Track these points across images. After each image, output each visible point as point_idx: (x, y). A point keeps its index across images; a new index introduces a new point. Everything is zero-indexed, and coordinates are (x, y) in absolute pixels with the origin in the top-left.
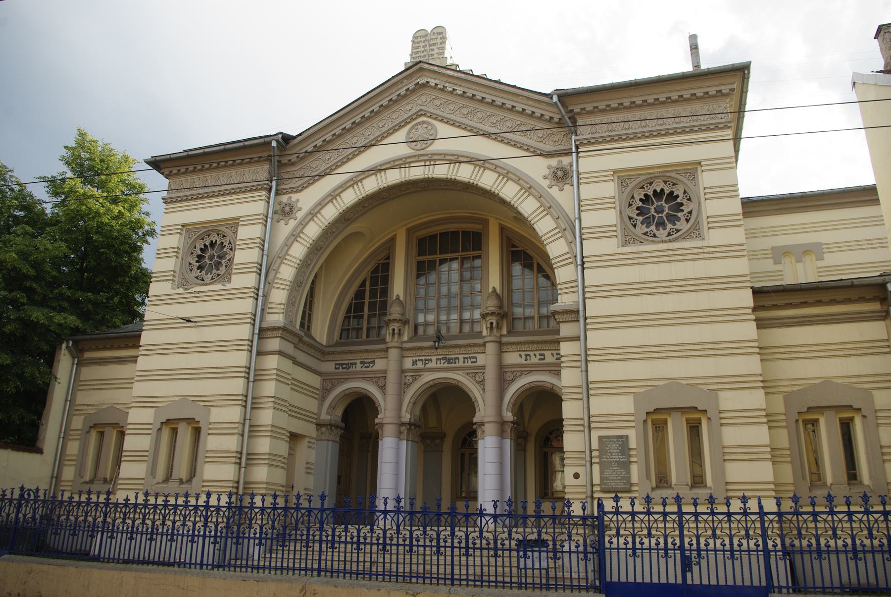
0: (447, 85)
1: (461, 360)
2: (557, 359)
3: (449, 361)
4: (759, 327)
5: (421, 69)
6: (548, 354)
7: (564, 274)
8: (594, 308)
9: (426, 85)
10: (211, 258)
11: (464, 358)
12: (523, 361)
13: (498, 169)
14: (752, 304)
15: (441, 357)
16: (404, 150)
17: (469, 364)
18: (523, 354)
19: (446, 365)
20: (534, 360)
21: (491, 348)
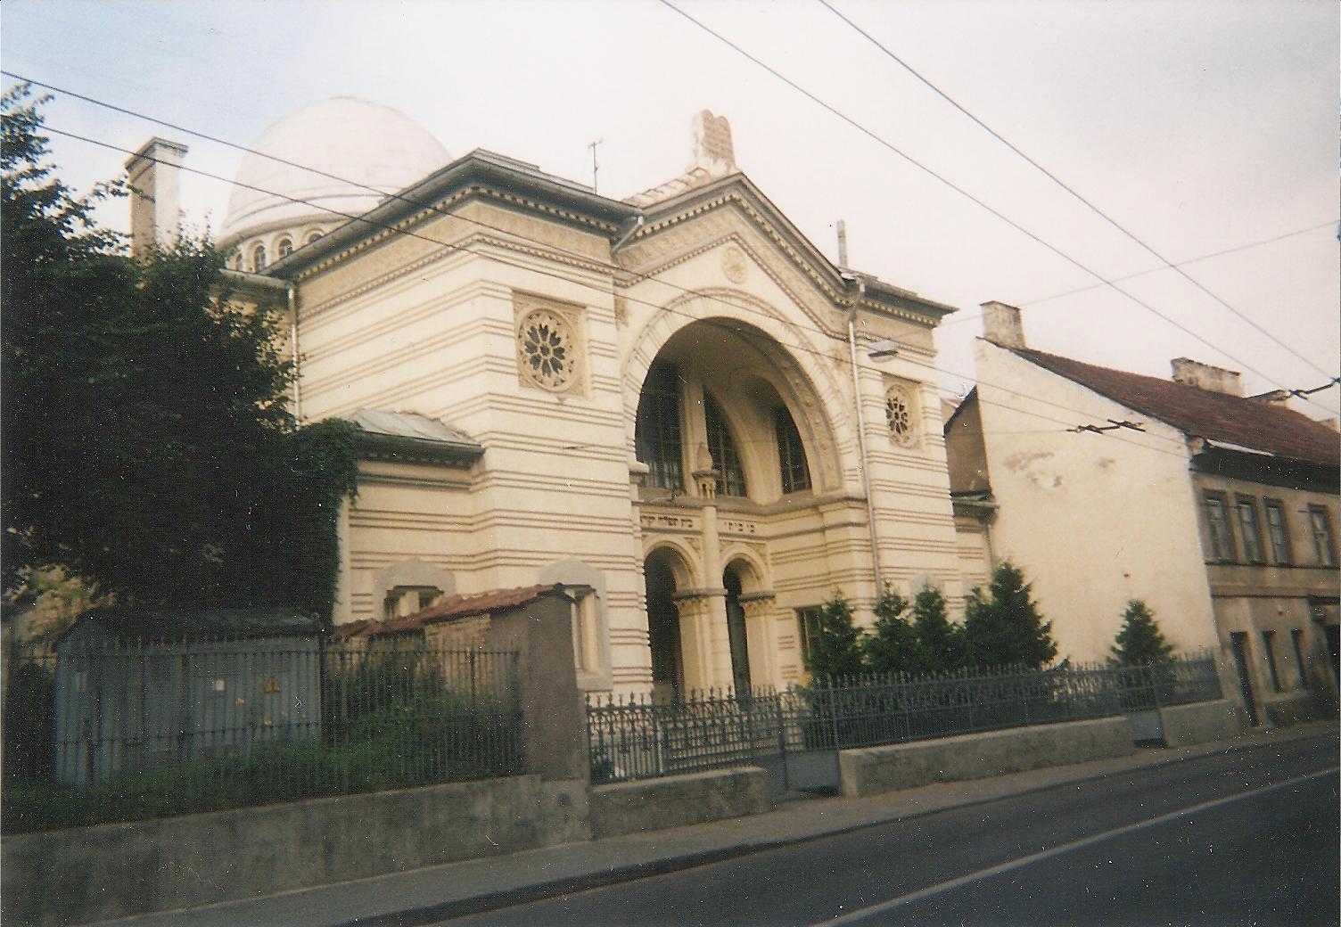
0: (758, 214)
1: (680, 522)
2: (752, 531)
3: (671, 521)
4: (958, 531)
5: (740, 181)
6: (745, 524)
7: (850, 461)
8: (881, 500)
9: (733, 200)
10: (545, 351)
11: (683, 520)
12: (726, 529)
13: (801, 336)
14: (952, 513)
15: (662, 516)
16: (721, 280)
17: (686, 527)
18: (727, 522)
19: (668, 527)
20: (735, 530)
21: (710, 512)
